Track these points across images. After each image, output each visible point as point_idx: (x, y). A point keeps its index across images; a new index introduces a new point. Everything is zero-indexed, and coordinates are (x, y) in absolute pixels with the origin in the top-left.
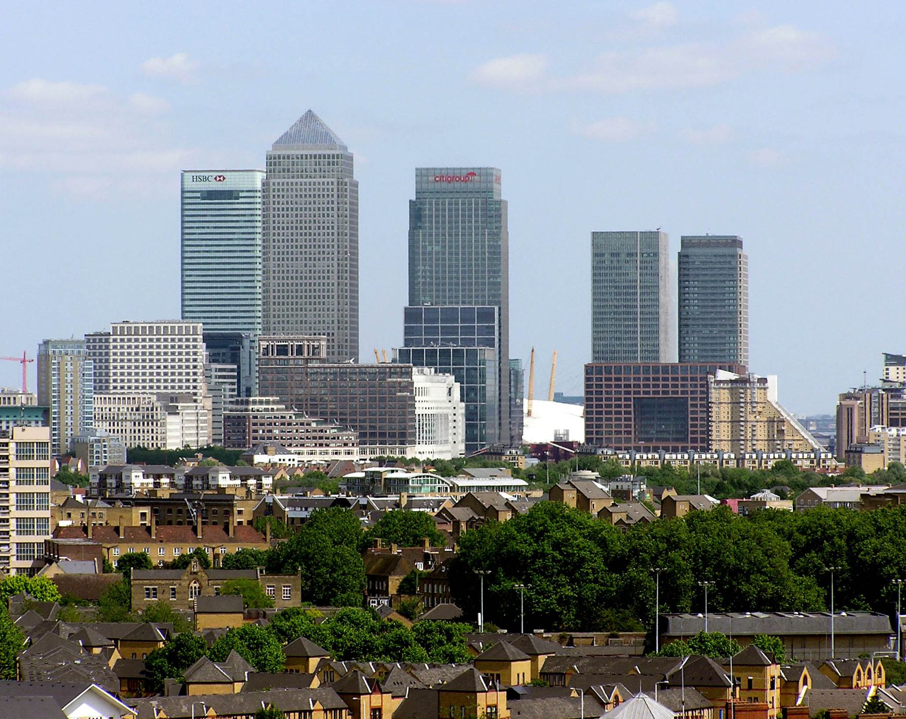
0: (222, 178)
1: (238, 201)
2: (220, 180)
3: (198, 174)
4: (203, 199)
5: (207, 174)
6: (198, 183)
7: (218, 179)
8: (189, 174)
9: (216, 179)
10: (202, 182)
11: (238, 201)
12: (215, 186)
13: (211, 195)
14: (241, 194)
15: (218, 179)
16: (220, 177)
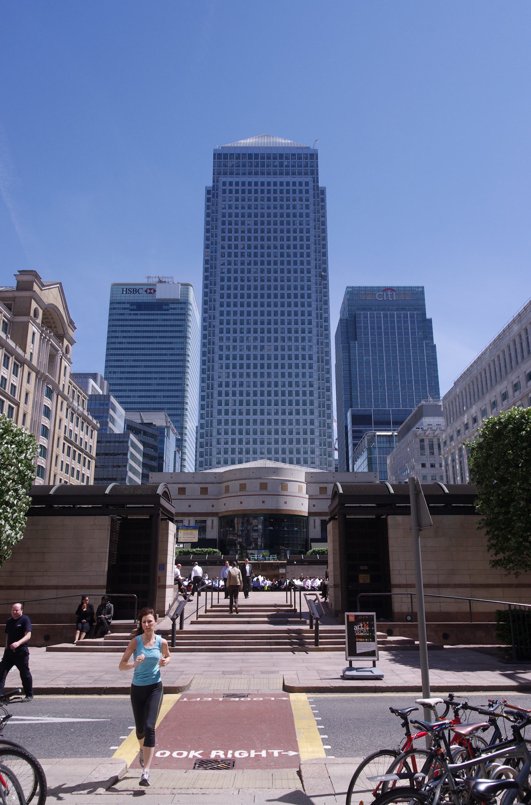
0: (152, 291)
1: (168, 312)
2: (150, 293)
3: (128, 287)
4: (132, 310)
5: (137, 287)
6: (127, 295)
7: (149, 291)
8: (120, 287)
9: (146, 291)
10: (132, 295)
11: (168, 312)
12: (144, 298)
13: (140, 306)
14: (171, 306)
15: (149, 291)
16: (150, 289)
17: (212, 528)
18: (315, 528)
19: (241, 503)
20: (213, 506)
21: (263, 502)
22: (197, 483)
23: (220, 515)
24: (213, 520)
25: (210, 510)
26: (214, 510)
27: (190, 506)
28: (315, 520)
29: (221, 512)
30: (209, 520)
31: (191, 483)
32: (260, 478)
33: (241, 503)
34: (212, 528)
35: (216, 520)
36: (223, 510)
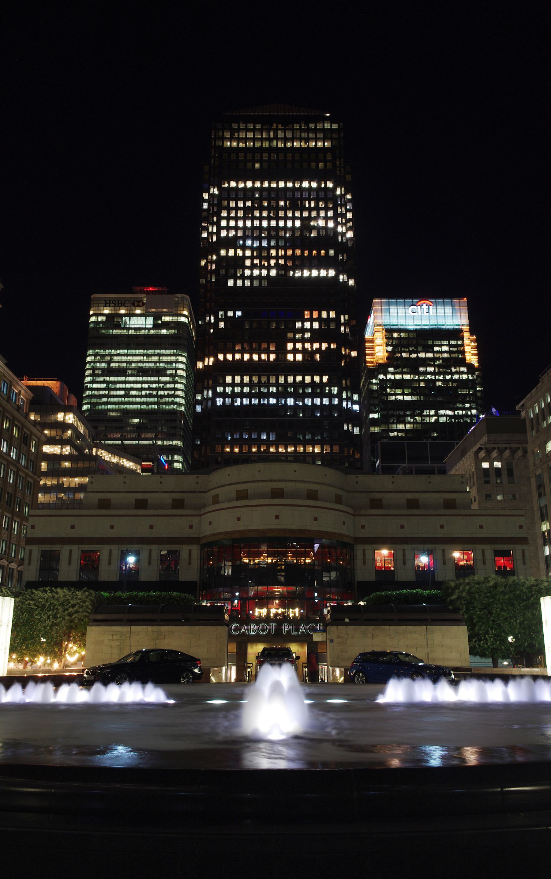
17: (190, 563)
18: (364, 563)
19: (239, 519)
20: (191, 527)
21: (277, 517)
22: (167, 492)
23: (203, 541)
24: (190, 551)
25: (187, 533)
26: (193, 534)
27: (151, 527)
28: (364, 551)
29: (204, 537)
30: (184, 550)
31: (157, 492)
32: (271, 481)
33: (239, 519)
34: (190, 563)
35: (195, 550)
36: (208, 533)
